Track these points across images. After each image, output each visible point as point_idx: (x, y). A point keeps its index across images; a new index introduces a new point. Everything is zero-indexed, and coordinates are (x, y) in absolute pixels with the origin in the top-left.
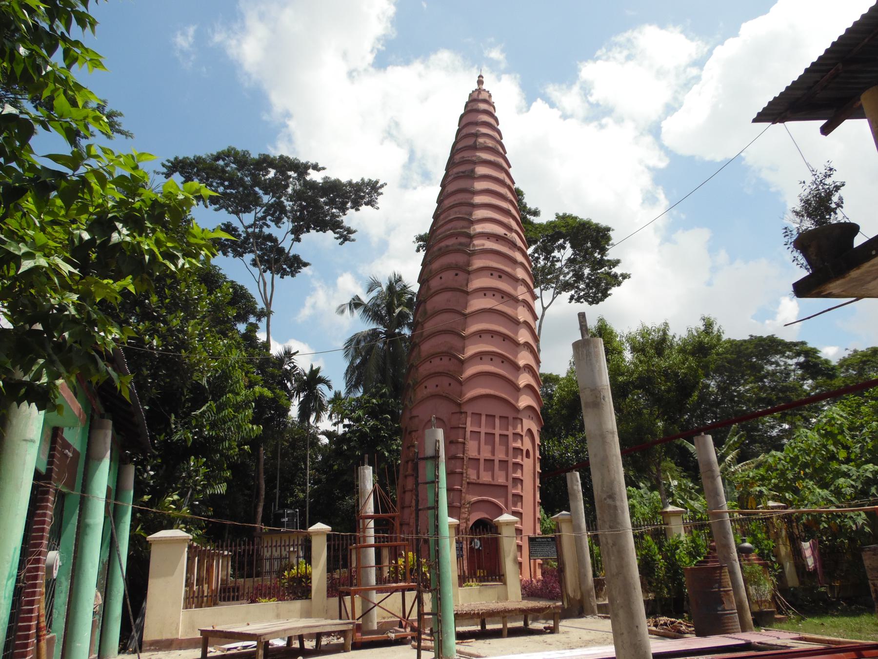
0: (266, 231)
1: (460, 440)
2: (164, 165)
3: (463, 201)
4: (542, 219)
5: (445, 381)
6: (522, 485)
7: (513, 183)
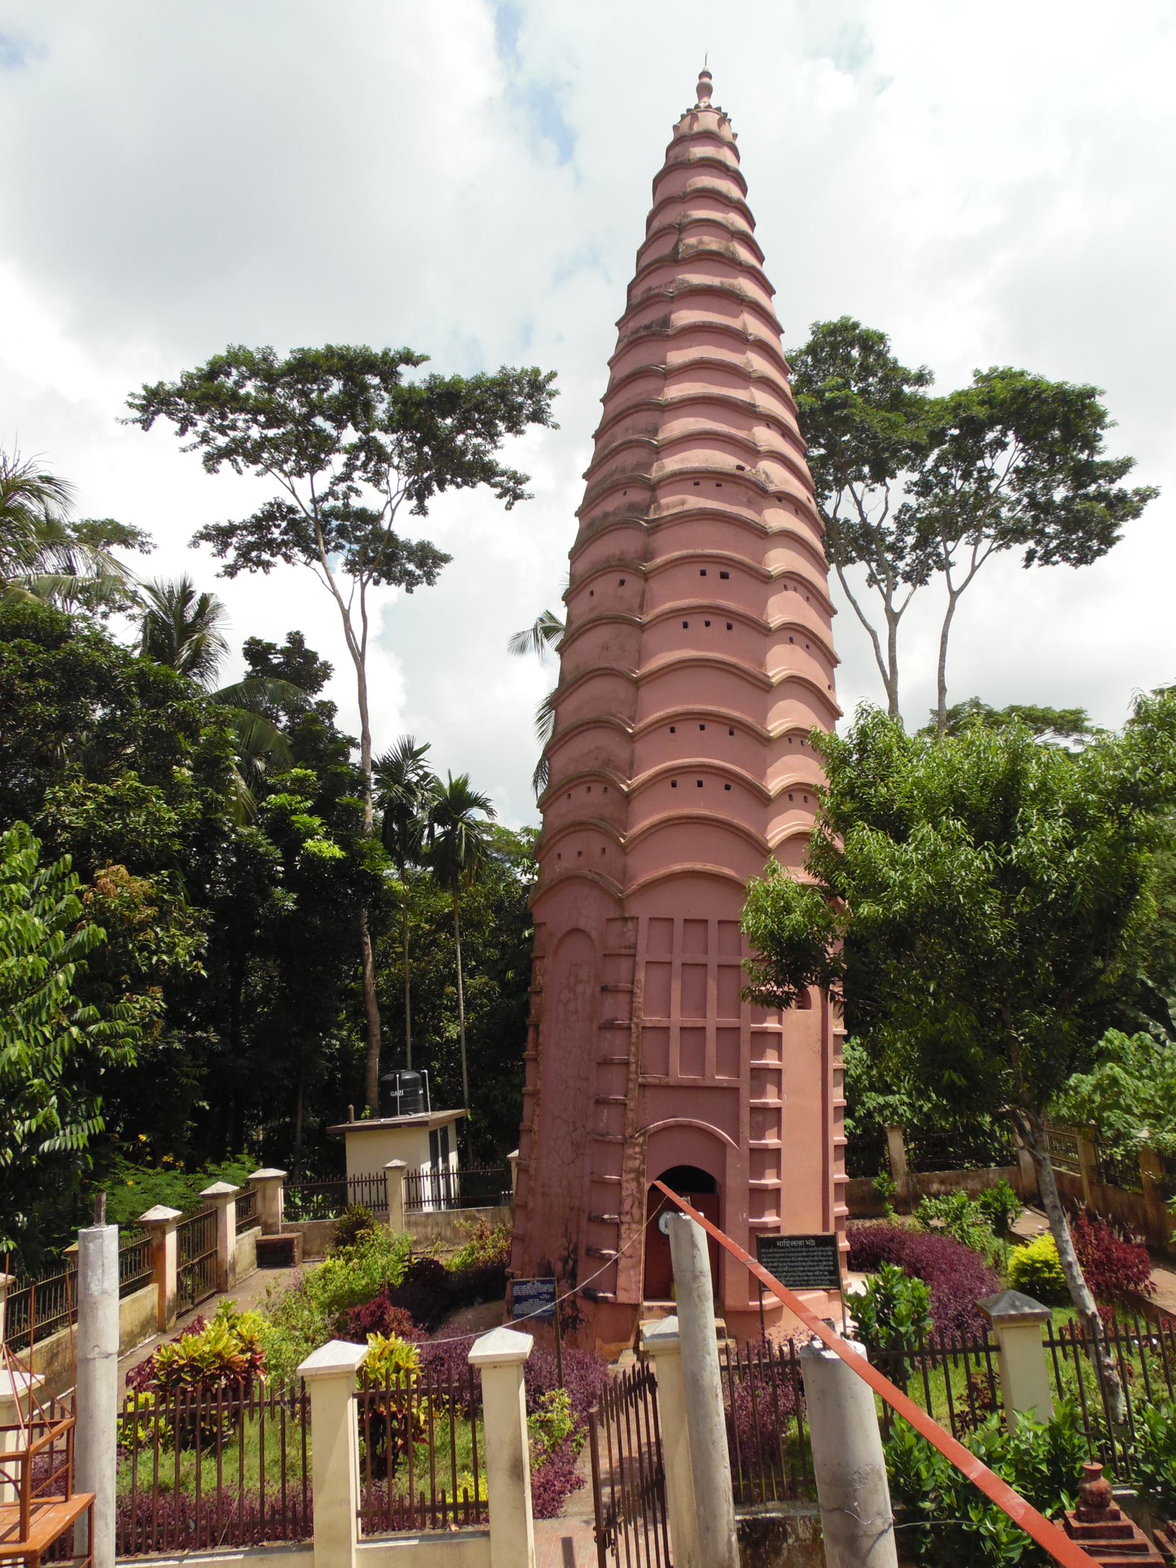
1: (622, 985)
2: (131, 405)
3: (629, 404)
4: (938, 391)
5: (593, 843)
6: (779, 1085)
7: (778, 330)
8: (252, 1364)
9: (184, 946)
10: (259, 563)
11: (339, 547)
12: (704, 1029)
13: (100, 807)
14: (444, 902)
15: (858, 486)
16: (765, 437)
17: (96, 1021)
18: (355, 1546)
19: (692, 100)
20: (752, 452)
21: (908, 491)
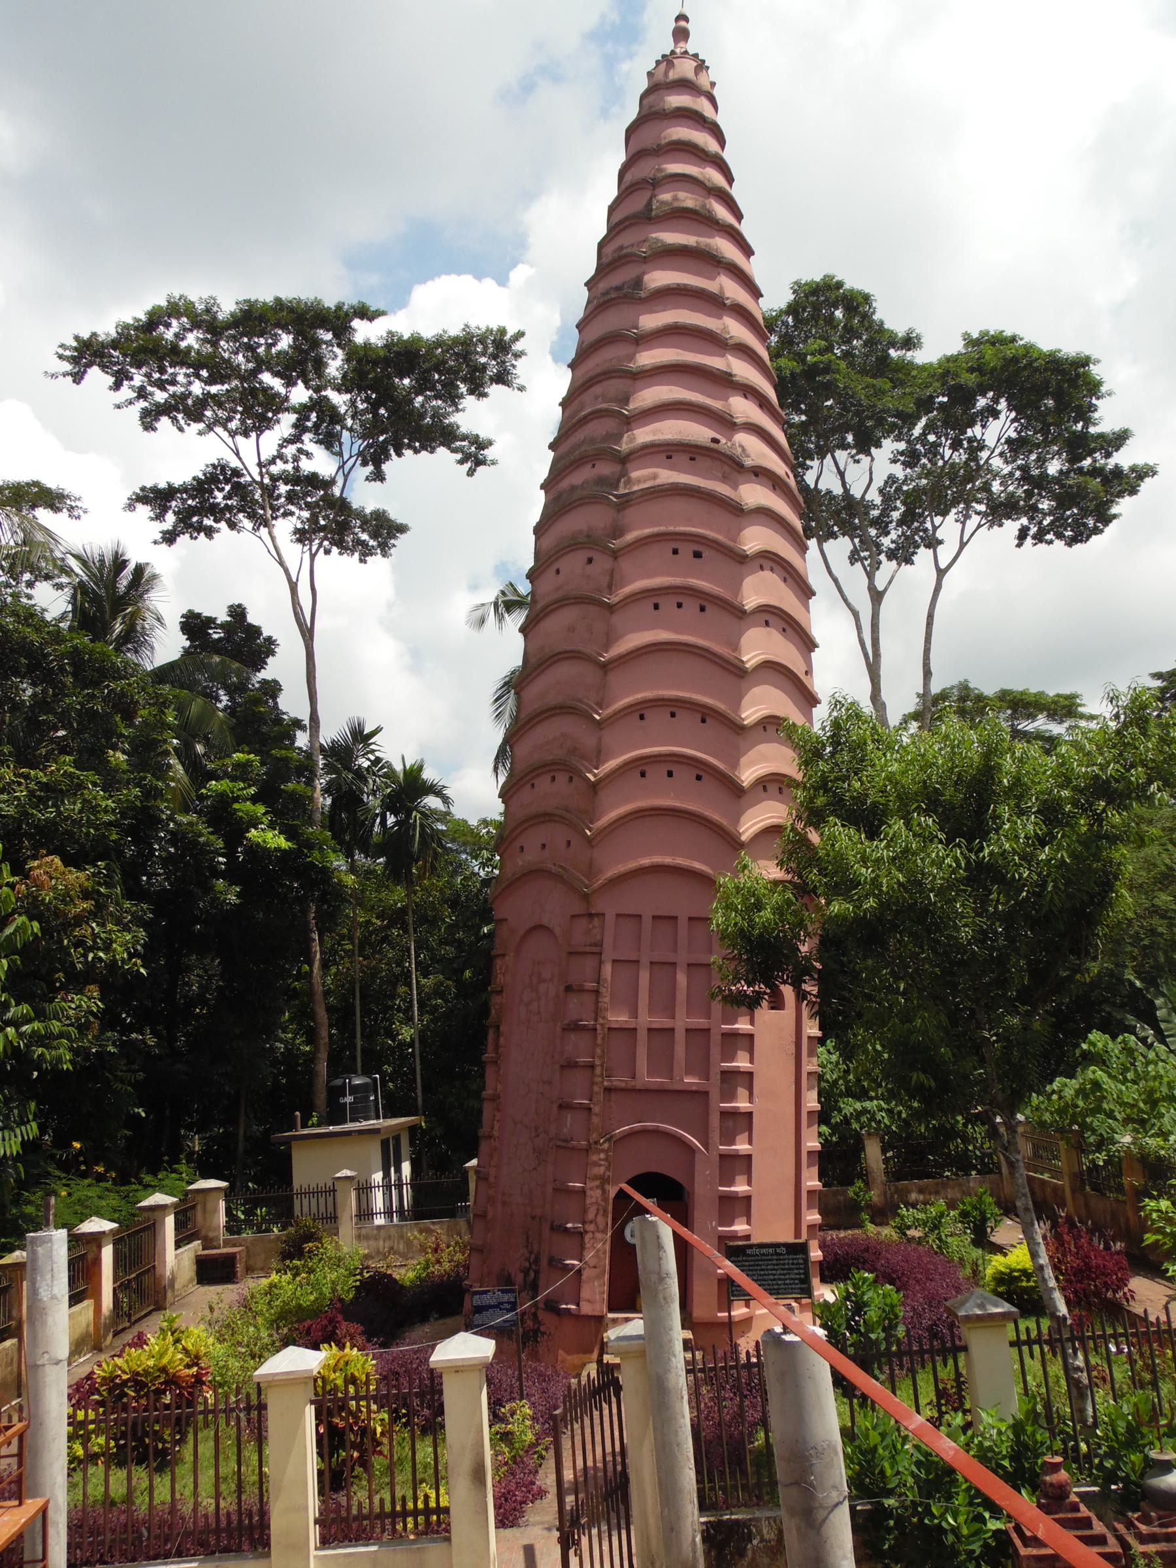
0: (307, 466)
2: (61, 357)
3: (599, 370)
4: (926, 355)
5: (557, 834)
6: (750, 1089)
7: (756, 293)
8: (198, 1380)
9: (122, 943)
10: (200, 528)
11: (287, 514)
12: (673, 1029)
13: (31, 793)
14: (397, 896)
15: (842, 455)
16: (742, 408)
17: (29, 1021)
18: (313, 1552)
19: (668, 45)
20: (727, 423)
21: (894, 461)
